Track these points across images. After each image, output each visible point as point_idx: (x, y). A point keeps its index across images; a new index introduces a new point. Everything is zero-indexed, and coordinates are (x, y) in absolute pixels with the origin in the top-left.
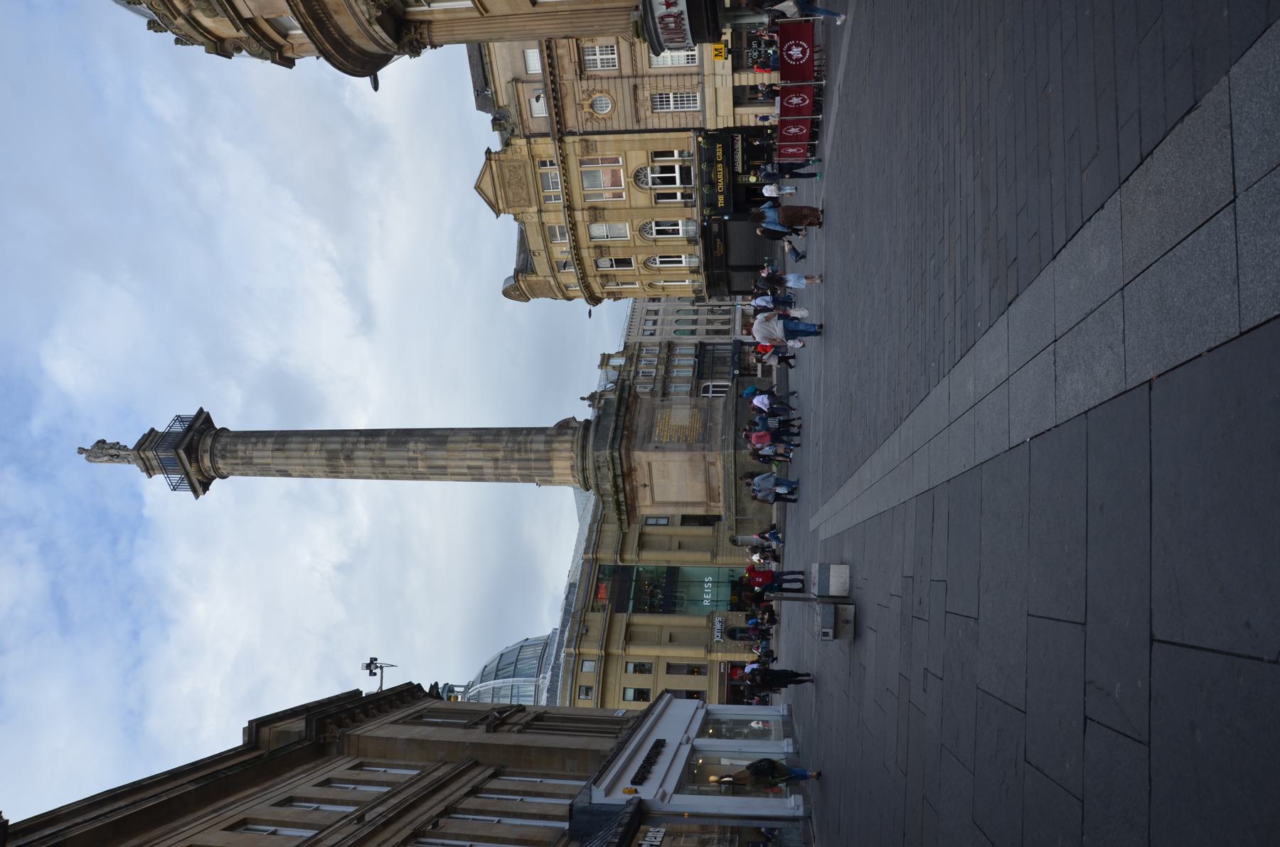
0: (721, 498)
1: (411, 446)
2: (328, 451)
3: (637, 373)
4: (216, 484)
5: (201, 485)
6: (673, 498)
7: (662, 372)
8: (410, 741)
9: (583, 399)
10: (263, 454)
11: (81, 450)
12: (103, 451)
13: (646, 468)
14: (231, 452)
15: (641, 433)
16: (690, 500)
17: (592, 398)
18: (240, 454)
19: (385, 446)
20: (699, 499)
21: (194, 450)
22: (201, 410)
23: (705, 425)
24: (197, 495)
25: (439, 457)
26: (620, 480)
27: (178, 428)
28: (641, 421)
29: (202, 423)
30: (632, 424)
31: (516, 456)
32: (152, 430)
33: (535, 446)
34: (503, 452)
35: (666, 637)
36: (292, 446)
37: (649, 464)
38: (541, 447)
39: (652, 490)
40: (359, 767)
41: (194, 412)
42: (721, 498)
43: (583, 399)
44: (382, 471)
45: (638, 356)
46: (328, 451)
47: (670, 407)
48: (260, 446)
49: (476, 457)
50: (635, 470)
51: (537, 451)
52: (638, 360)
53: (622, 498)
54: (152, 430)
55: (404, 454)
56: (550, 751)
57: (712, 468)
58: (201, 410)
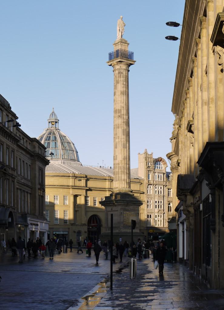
1: (123, 137)
2: (121, 110)
8: (35, 174)
14: (120, 76)
15: (126, 208)
18: (120, 79)
19: (123, 128)
22: (135, 62)
25: (120, 147)
30: (129, 205)
31: (120, 170)
33: (123, 176)
36: (122, 97)
37: (117, 211)
38: (123, 178)
40: (30, 165)
41: (134, 60)
44: (116, 127)
46: (121, 110)
48: (122, 86)
51: (121, 177)
53: (108, 203)
54: (128, 44)
55: (120, 135)
56: (35, 203)
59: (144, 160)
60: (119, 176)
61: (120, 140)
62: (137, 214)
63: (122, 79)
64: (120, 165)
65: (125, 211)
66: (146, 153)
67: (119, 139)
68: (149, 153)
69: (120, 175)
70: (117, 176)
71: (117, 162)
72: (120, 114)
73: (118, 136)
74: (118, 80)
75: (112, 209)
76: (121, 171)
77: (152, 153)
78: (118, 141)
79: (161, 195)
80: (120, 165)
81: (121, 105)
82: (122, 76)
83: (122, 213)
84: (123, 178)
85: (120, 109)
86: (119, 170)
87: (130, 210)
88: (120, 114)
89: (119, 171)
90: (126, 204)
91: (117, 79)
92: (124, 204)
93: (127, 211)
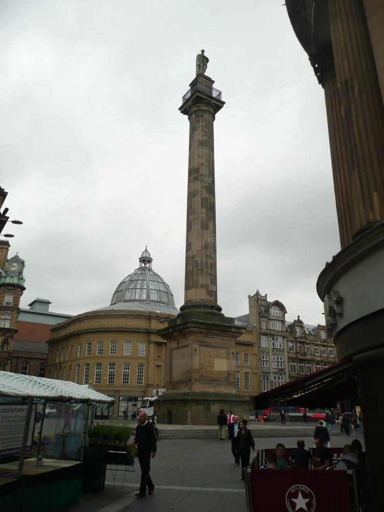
0: (172, 391)
2: (198, 168)
3: (317, 345)
4: (186, 117)
5: (184, 110)
6: (174, 362)
7: (318, 359)
9: (299, 317)
10: (199, 136)
11: (203, 51)
12: (202, 61)
13: (186, 344)
14: (199, 119)
15: (207, 340)
16: (173, 371)
17: (299, 323)
18: (197, 125)
20: (173, 378)
21: (202, 103)
22: (224, 103)
23: (214, 380)
24: (180, 109)
25: (197, 227)
26: (177, 329)
27: (215, 94)
28: (217, 340)
29: (218, 105)
30: (213, 334)
32: (213, 82)
34: (201, 262)
35: (159, 364)
37: (187, 346)
39: (176, 348)
41: (223, 100)
42: (172, 391)
43: (299, 317)
45: (327, 346)
46: (198, 168)
47: (228, 358)
49: (197, 245)
50: (185, 337)
52: (324, 346)
57: (185, 384)
58: (224, 103)
59: (256, 303)
60: (193, 279)
61: (196, 216)
62: (231, 356)
63: (201, 124)
64: (198, 259)
65: (203, 346)
66: (257, 294)
67: (194, 214)
68: (263, 295)
69: (195, 278)
70: (191, 278)
71: (190, 253)
72: (196, 175)
73: (194, 210)
74: (196, 126)
75: (178, 344)
76: (197, 270)
77: (266, 295)
78: (194, 217)
79: (279, 349)
80: (195, 260)
81: (199, 161)
82: (201, 121)
83: (196, 350)
84: (200, 282)
85: (197, 167)
86: (193, 267)
87: (214, 344)
88: (196, 175)
89: (193, 270)
90: (205, 330)
91: (194, 126)
92: (202, 330)
93: (207, 346)
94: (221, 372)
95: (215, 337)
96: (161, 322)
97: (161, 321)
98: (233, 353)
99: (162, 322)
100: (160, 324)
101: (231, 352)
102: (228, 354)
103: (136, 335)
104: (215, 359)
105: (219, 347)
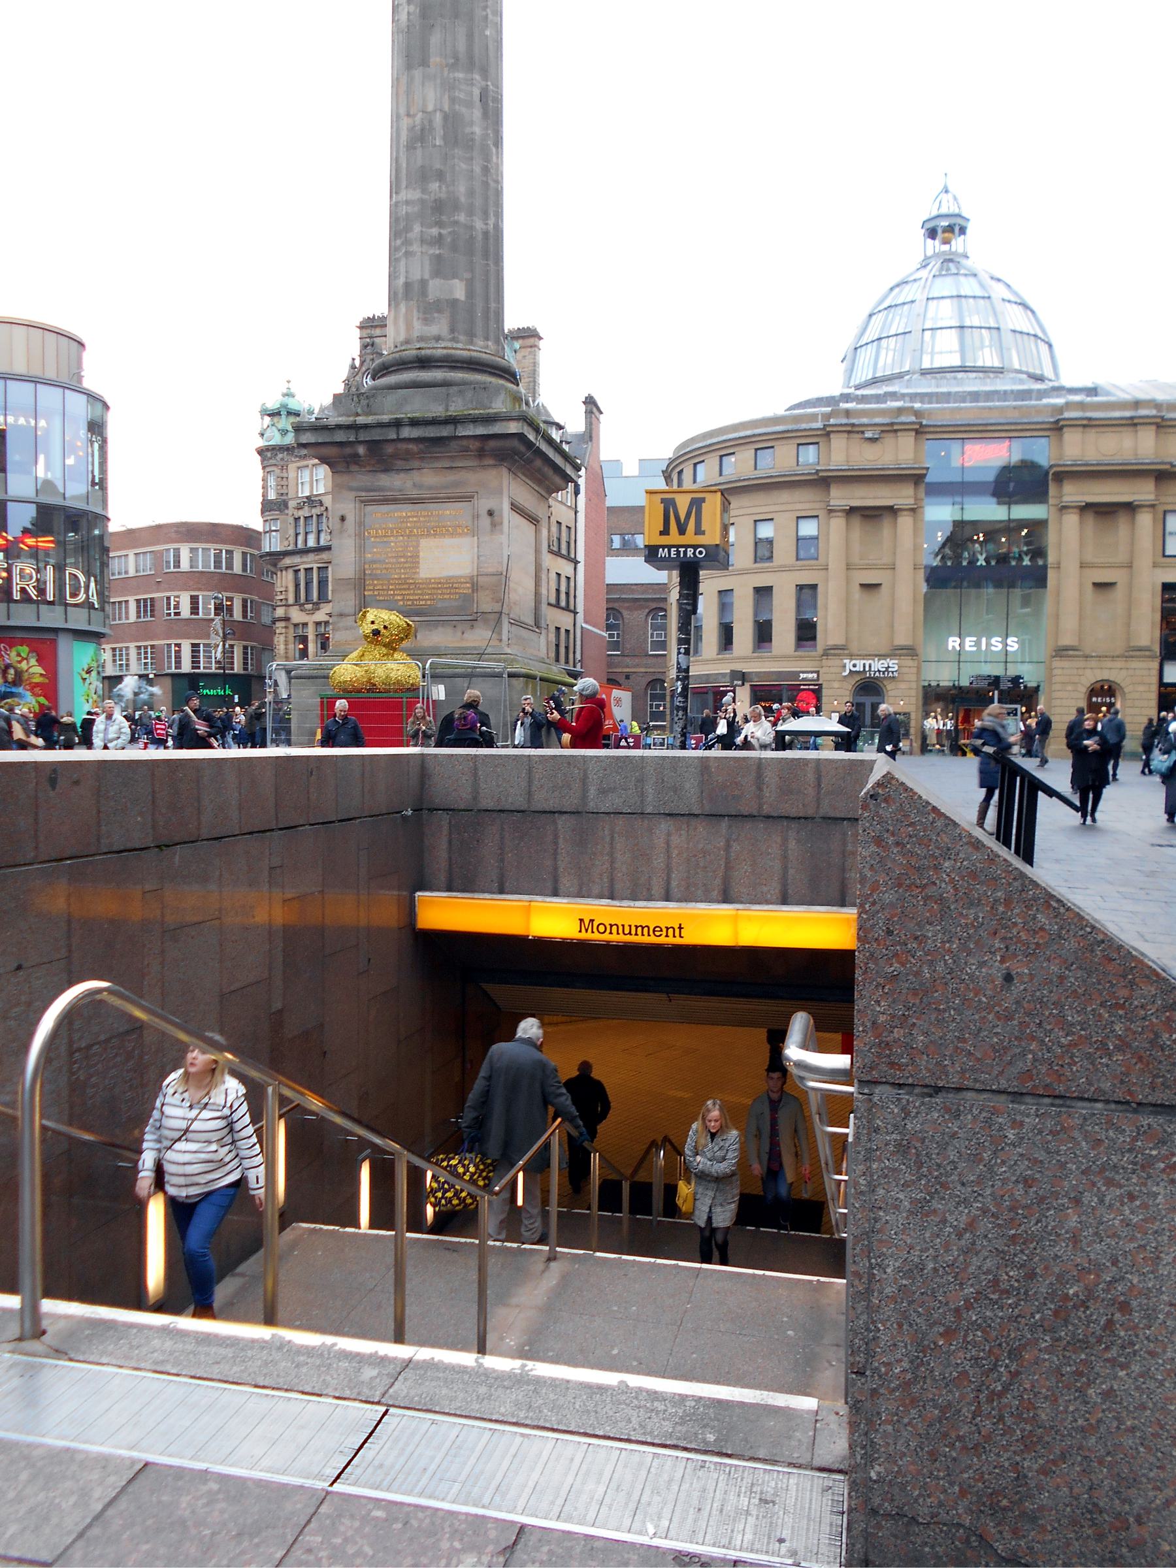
47: (474, 532)
62: (486, 521)
83: (343, 519)
92: (348, 450)
93: (386, 501)
94: (449, 584)
95: (416, 464)
96: (873, 440)
97: (868, 435)
98: (491, 513)
99: (873, 440)
100: (867, 446)
101: (483, 512)
102: (476, 517)
103: (785, 496)
104: (424, 543)
105: (435, 500)
